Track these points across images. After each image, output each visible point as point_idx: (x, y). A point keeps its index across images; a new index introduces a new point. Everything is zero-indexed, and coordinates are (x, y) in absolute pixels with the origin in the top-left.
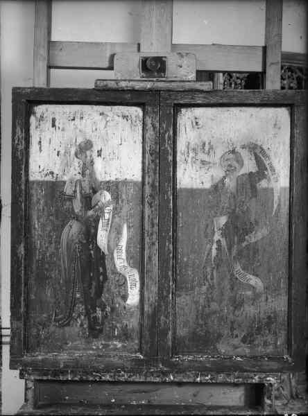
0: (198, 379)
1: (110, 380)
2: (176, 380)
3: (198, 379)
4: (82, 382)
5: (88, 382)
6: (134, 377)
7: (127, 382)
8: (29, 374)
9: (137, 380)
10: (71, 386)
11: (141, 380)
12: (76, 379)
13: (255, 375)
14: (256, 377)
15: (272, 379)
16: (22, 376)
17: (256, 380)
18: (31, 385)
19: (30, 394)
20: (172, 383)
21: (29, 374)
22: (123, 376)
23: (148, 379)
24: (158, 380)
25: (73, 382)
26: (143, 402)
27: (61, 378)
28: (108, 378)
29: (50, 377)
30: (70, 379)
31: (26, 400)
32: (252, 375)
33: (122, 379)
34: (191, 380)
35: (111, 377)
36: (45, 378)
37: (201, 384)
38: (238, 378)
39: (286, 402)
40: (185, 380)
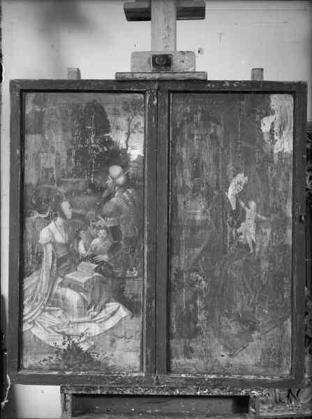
1: (131, 393)
2: (181, 393)
6: (149, 391)
8: (68, 390)
11: (154, 394)
12: (104, 393)
15: (255, 393)
17: (243, 393)
18: (69, 398)
19: (69, 405)
20: (179, 396)
23: (160, 393)
24: (167, 393)
26: (157, 411)
27: (92, 392)
29: (83, 392)
30: (99, 393)
31: (64, 409)
33: (139, 393)
34: (193, 394)
36: (80, 392)
37: (201, 397)
38: (229, 391)
39: (271, 405)
40: (188, 394)
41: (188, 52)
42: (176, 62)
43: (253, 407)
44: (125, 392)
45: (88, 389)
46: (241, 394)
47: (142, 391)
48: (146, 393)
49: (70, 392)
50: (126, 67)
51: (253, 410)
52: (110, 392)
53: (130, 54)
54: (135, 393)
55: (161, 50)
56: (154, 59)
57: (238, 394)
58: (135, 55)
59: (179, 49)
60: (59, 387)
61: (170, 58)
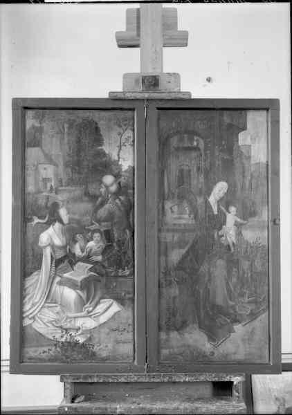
4: (104, 383)
7: (136, 383)
9: (144, 381)
11: (147, 381)
13: (227, 376)
14: (228, 377)
16: (62, 380)
18: (68, 386)
21: (67, 379)
24: (158, 380)
25: (98, 383)
28: (123, 380)
33: (132, 380)
35: (125, 379)
41: (174, 73)
42: (163, 84)
43: (237, 391)
44: (120, 380)
45: (85, 377)
46: (226, 380)
47: (136, 379)
49: (69, 381)
50: (118, 87)
51: (237, 394)
52: (106, 381)
54: (129, 380)
55: (150, 72)
58: (126, 76)
59: (165, 71)
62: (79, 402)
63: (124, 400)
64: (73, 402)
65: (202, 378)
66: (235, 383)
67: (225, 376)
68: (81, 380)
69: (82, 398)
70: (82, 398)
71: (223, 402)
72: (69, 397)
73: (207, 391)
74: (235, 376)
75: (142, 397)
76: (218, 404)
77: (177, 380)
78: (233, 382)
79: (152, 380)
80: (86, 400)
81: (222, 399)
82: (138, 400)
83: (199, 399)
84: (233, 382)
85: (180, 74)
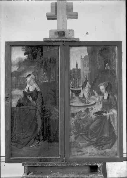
0: (78, 165)
3: (78, 165)
5: (43, 166)
8: (25, 165)
9: (59, 165)
10: (37, 168)
12: (40, 165)
16: (23, 165)
22: (54, 164)
24: (65, 165)
27: (35, 165)
32: (94, 163)
36: (30, 166)
42: (67, 33)
43: (99, 170)
44: (48, 165)
45: (33, 164)
46: (95, 165)
48: (57, 165)
49: (26, 165)
50: (47, 36)
51: (99, 171)
52: (42, 165)
53: (49, 31)
55: (61, 29)
56: (58, 33)
57: (93, 165)
58: (51, 31)
59: (68, 29)
60: (22, 164)
61: (64, 32)
62: (30, 175)
63: (50, 174)
64: (28, 175)
65: (84, 164)
66: (99, 166)
67: (94, 163)
68: (32, 165)
69: (32, 173)
70: (32, 173)
71: (94, 175)
72: (26, 173)
73: (87, 170)
74: (99, 163)
75: (58, 172)
76: (91, 175)
77: (73, 165)
78: (98, 166)
79: (62, 165)
80: (33, 174)
81: (93, 173)
82: (56, 174)
83: (83, 174)
84: (98, 166)
85: (74, 31)
